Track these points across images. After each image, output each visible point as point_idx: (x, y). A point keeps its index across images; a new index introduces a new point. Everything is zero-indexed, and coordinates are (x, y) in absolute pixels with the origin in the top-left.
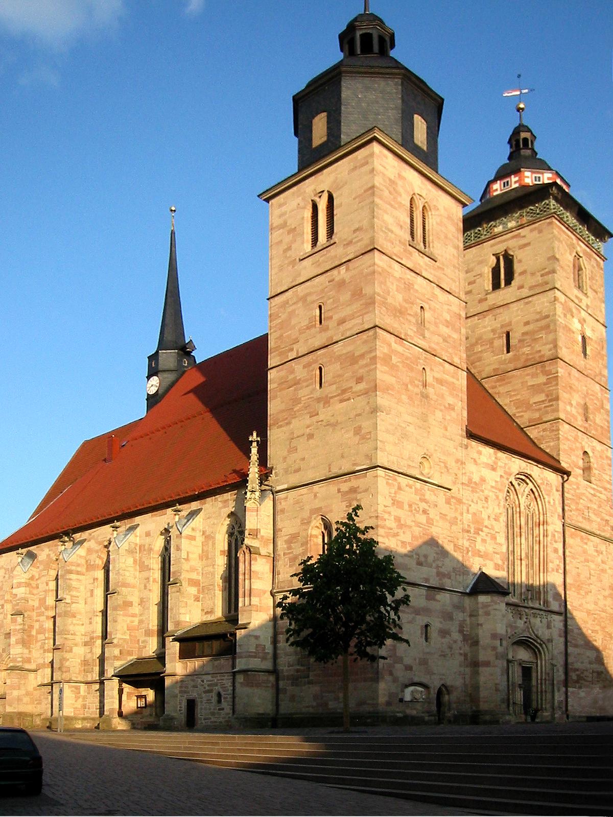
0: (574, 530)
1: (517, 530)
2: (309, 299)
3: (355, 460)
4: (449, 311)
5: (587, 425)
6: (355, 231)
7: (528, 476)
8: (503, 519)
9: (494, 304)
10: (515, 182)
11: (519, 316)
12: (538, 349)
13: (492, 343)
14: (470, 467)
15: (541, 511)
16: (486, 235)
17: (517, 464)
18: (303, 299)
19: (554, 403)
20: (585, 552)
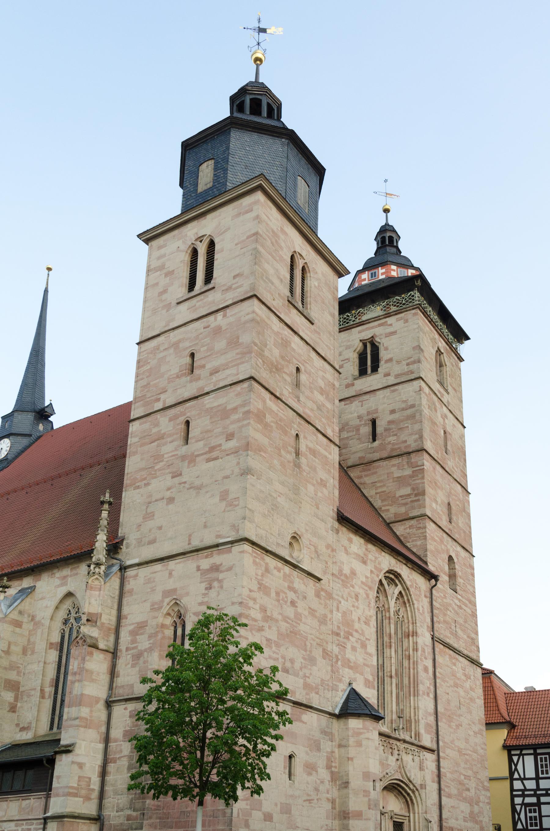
0: (442, 646)
1: (386, 639)
2: (181, 345)
3: (219, 531)
4: (323, 378)
5: (451, 527)
6: (234, 277)
7: (398, 576)
8: (373, 623)
9: (361, 390)
10: (382, 274)
11: (384, 403)
12: (404, 439)
13: (358, 430)
14: (342, 556)
15: (410, 619)
16: (354, 321)
17: (387, 562)
18: (176, 345)
19: (421, 497)
20: (454, 675)
